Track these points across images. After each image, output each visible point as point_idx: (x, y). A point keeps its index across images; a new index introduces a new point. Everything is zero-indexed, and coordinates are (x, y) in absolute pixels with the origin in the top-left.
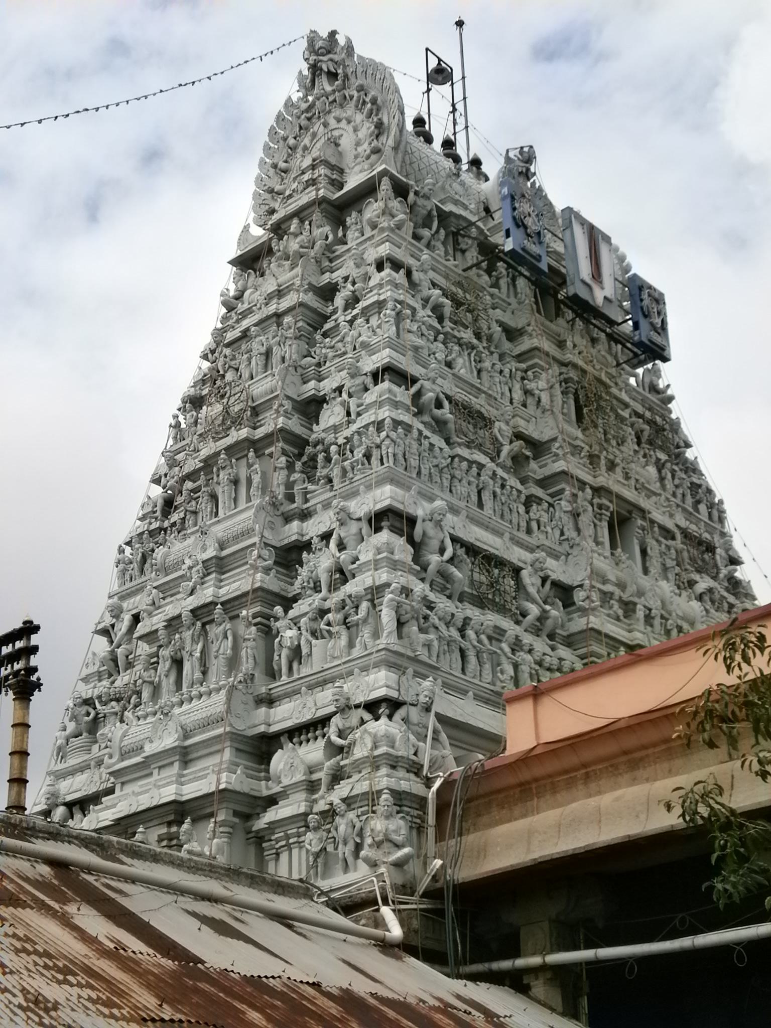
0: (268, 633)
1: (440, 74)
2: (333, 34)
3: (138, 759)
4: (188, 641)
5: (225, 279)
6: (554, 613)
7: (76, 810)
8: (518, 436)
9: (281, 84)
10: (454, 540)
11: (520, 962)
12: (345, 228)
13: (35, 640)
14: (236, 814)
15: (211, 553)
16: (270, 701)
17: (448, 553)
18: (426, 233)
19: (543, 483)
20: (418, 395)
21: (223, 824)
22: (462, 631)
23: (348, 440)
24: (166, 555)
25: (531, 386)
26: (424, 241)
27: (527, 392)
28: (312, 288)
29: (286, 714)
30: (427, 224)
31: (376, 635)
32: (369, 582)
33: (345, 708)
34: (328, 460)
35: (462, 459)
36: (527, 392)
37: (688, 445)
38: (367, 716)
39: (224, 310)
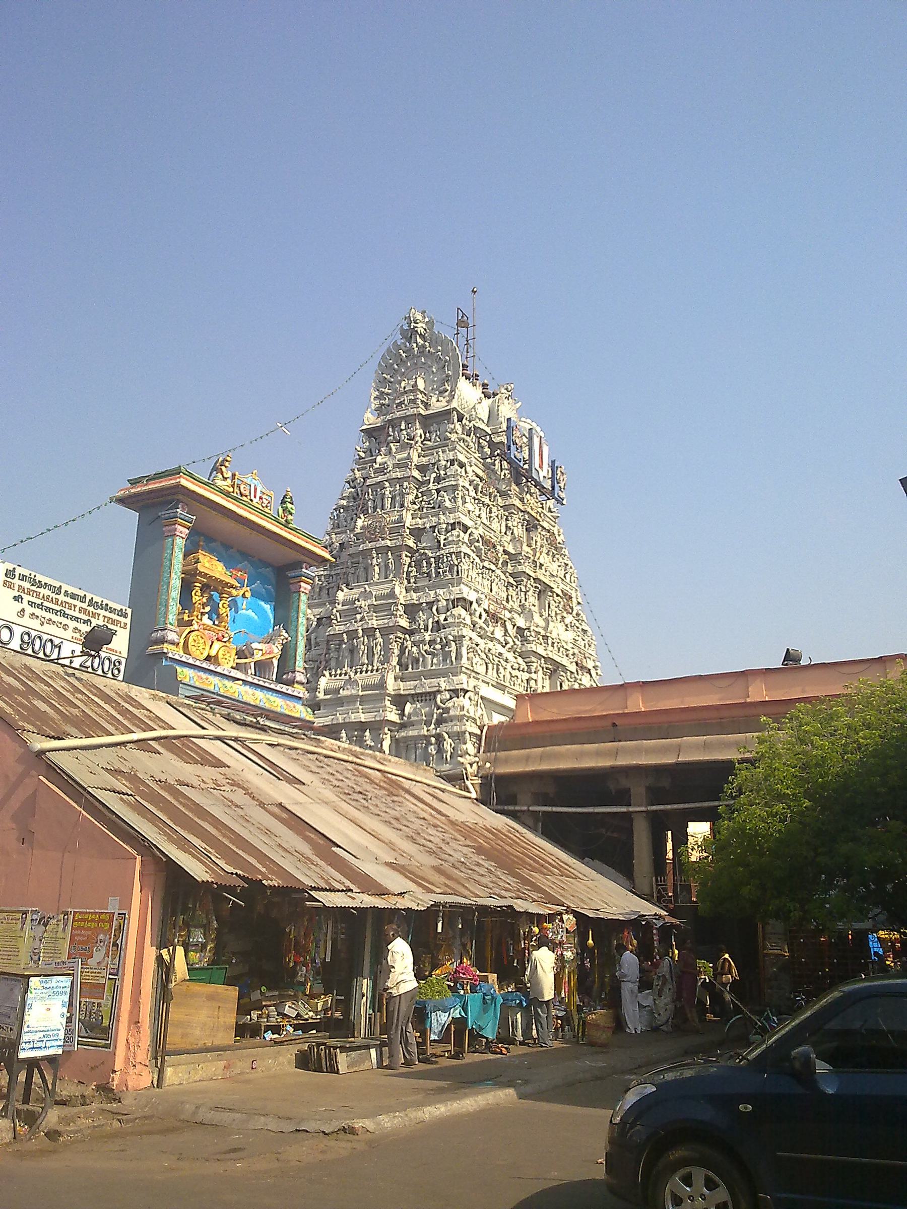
1: (462, 323)
25: (510, 524)
36: (506, 526)
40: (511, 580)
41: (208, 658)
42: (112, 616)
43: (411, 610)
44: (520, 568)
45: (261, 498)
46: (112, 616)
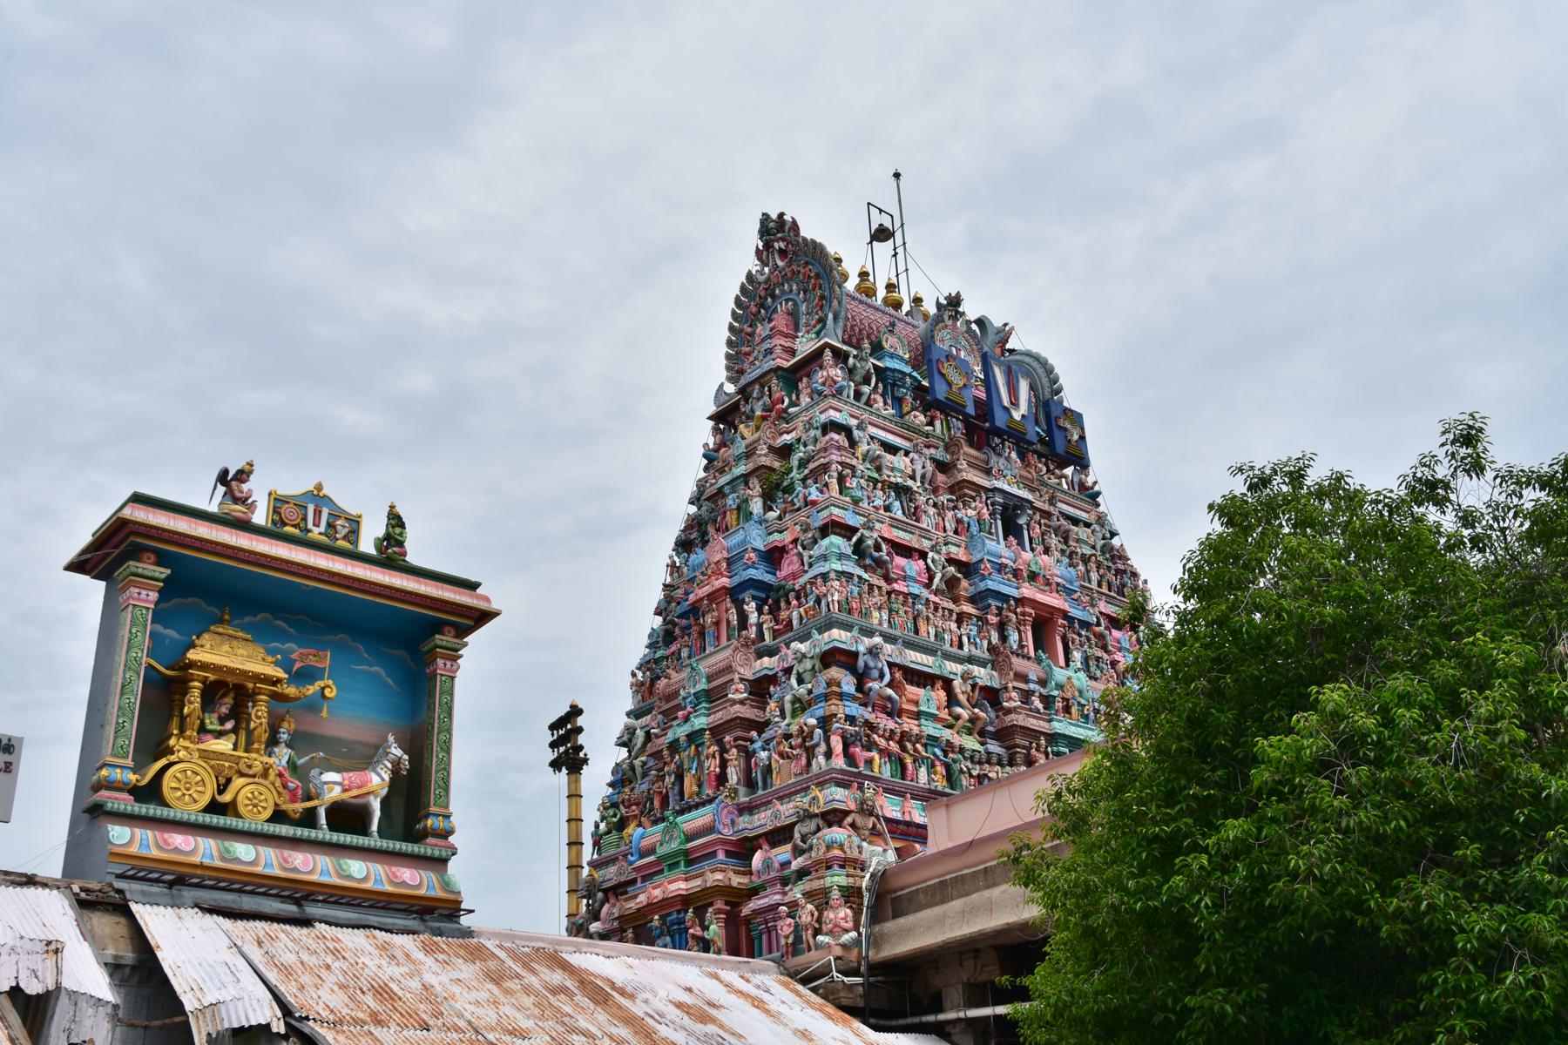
0: (749, 755)
2: (781, 215)
3: (652, 858)
4: (686, 762)
5: (704, 434)
6: (982, 714)
7: (610, 894)
8: (951, 561)
9: (740, 259)
10: (891, 665)
11: (942, 1017)
13: (580, 721)
14: (727, 903)
15: (703, 685)
16: (749, 809)
17: (887, 678)
18: (866, 389)
19: (972, 600)
20: (861, 541)
22: (900, 743)
23: (804, 588)
26: (864, 399)
27: (959, 521)
28: (771, 449)
29: (763, 820)
30: (867, 381)
31: (829, 754)
32: (820, 713)
34: (788, 603)
35: (898, 593)
37: (1113, 534)
38: (821, 823)
39: (705, 462)
40: (968, 608)
41: (214, 807)
43: (761, 688)
44: (982, 586)
45: (329, 525)
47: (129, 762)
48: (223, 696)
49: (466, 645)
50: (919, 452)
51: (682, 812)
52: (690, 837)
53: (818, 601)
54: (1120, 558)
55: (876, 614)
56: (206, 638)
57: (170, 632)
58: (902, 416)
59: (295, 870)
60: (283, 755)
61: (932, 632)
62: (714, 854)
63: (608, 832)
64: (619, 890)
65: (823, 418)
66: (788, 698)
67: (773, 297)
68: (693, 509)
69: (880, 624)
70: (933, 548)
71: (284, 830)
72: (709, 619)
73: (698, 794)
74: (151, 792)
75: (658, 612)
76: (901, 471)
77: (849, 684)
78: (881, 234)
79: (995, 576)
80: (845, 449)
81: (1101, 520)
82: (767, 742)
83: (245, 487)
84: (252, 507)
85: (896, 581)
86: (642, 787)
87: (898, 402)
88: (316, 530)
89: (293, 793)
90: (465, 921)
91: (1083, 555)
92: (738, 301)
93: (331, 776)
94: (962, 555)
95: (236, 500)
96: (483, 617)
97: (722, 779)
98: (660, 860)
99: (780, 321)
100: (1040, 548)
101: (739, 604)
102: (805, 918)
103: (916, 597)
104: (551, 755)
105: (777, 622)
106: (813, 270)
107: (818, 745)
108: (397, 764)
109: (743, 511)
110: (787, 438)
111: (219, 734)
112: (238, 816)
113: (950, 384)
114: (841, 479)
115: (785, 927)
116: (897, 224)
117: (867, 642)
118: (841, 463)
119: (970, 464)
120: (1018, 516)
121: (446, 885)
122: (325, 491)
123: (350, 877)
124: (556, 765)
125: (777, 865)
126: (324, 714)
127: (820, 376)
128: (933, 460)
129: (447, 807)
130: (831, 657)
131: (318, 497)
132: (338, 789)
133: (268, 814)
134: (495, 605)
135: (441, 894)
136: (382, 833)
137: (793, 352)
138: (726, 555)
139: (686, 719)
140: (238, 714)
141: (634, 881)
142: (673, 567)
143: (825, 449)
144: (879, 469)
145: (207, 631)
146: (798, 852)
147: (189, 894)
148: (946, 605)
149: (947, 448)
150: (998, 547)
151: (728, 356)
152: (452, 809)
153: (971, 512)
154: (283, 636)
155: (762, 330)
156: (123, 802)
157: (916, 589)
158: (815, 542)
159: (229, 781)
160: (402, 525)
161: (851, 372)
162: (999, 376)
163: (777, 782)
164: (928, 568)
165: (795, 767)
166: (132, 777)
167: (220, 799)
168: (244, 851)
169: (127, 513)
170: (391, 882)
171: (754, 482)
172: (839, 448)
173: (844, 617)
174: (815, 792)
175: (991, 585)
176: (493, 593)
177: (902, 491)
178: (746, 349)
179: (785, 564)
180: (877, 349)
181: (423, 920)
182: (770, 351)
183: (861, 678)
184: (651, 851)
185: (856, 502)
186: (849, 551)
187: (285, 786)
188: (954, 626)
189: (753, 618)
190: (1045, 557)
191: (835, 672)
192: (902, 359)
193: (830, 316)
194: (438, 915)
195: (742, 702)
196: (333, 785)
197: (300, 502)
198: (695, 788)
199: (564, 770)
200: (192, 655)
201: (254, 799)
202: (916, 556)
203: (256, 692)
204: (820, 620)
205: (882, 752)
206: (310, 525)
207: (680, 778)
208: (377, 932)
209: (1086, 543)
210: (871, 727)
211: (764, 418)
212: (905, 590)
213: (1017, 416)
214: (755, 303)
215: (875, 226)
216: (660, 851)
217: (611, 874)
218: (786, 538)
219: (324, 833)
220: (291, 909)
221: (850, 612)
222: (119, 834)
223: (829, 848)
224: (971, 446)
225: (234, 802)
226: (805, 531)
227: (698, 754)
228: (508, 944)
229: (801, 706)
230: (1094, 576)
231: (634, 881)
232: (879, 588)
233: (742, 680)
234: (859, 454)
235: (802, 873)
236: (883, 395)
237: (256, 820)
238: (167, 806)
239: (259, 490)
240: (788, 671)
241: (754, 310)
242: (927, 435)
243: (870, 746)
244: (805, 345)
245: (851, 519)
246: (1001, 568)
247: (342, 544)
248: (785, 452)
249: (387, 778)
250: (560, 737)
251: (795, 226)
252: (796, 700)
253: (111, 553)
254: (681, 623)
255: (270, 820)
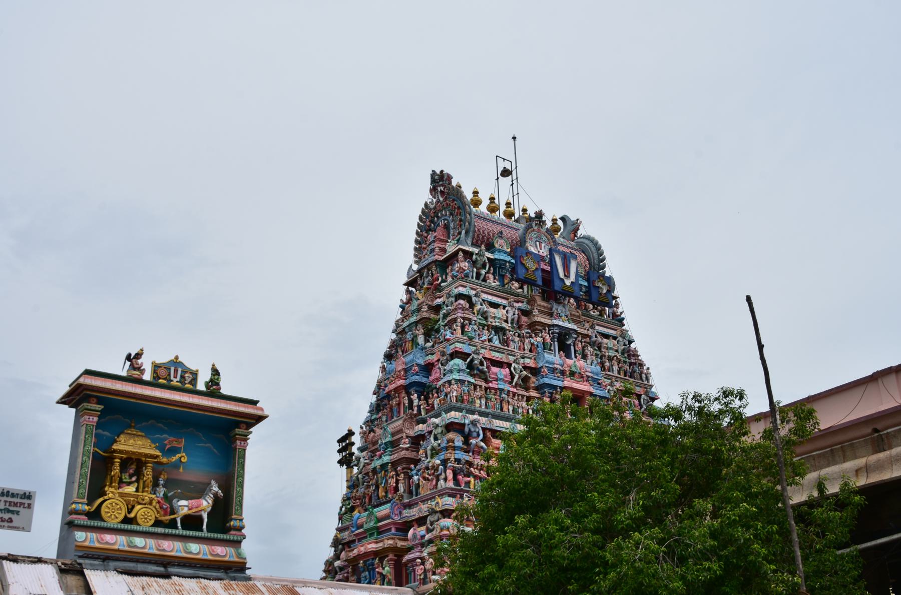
2: (442, 172)
8: (525, 368)
9: (423, 195)
10: (484, 429)
12: (447, 274)
14: (395, 556)
16: (409, 506)
18: (483, 272)
19: (537, 389)
21: (391, 560)
24: (374, 437)
26: (482, 277)
27: (532, 344)
30: (484, 266)
31: (445, 479)
32: (442, 457)
33: (433, 512)
37: (630, 342)
38: (440, 516)
40: (533, 393)
41: (126, 520)
42: (15, 500)
43: (417, 441)
44: (542, 381)
45: (182, 377)
46: (15, 500)
47: (85, 501)
48: (132, 464)
49: (251, 432)
50: (512, 306)
51: (377, 506)
52: (380, 520)
53: (446, 395)
54: (634, 355)
55: (478, 401)
56: (122, 438)
57: (106, 433)
58: (503, 285)
59: (164, 550)
60: (161, 491)
61: (511, 408)
62: (390, 530)
63: (346, 513)
64: (349, 545)
65: (456, 291)
66: (429, 448)
67: (438, 217)
68: (394, 336)
69: (481, 406)
70: (515, 361)
71: (160, 530)
72: (394, 402)
73: (386, 496)
74: (96, 515)
75: (374, 394)
76: (500, 319)
77: (459, 441)
78: (506, 173)
79: (550, 375)
80: (466, 309)
81: (624, 334)
82: (419, 471)
83: (140, 361)
84: (142, 372)
85: (491, 382)
86: (361, 490)
87: (502, 277)
88: (175, 380)
89: (165, 510)
90: (248, 572)
91: (609, 356)
92: (421, 218)
93: (183, 502)
94: (530, 362)
95: (135, 369)
96: (260, 419)
97: (396, 489)
98: (366, 531)
99: (439, 233)
100: (579, 357)
101: (409, 394)
102: (428, 566)
103: (502, 390)
104: (338, 457)
105: (428, 405)
106: (457, 203)
107: (441, 474)
108: (216, 495)
109: (414, 341)
110: (439, 301)
111: (129, 484)
112: (138, 524)
113: (527, 269)
114: (463, 327)
115: (419, 570)
116: (514, 167)
117: (473, 417)
118: (464, 318)
119: (540, 311)
120: (567, 340)
121: (239, 555)
122: (180, 360)
123: (191, 553)
124: (341, 462)
125: (419, 537)
126: (181, 470)
127: (457, 266)
128: (519, 309)
129: (241, 515)
130: (451, 427)
131: (176, 363)
132: (186, 509)
133: (152, 522)
134: (266, 413)
135: (236, 559)
136: (209, 530)
137: (444, 250)
138: (404, 367)
139: (380, 457)
140: (139, 474)
141: (353, 541)
142: (383, 369)
143: (456, 310)
144: (486, 319)
145: (122, 432)
146: (429, 531)
147: (112, 564)
148: (521, 392)
149: (528, 303)
150: (555, 358)
151: (416, 249)
152: (244, 516)
153: (539, 339)
154: (162, 432)
155: (431, 237)
156: (83, 520)
157: (502, 386)
158: (447, 363)
159: (133, 507)
160: (218, 374)
161: (474, 263)
162: (558, 260)
163: (423, 492)
164: (511, 373)
165: (429, 485)
166: (86, 508)
167: (129, 516)
168: (139, 541)
169: (81, 380)
170: (211, 554)
171: (420, 326)
172: (463, 309)
173: (459, 405)
174: (438, 500)
175: (546, 380)
176: (265, 406)
177: (499, 330)
178: (424, 246)
179: (433, 373)
180: (490, 247)
181: (226, 573)
182: (433, 250)
183: (467, 438)
184: (361, 526)
185: (471, 339)
186: (464, 367)
187: (161, 507)
188: (524, 404)
189: (416, 403)
190: (582, 362)
191: (451, 435)
192: (505, 252)
193: (463, 232)
194: (235, 570)
195: (407, 449)
196: (184, 506)
197: (166, 367)
198: (384, 494)
199: (345, 467)
200: (115, 447)
201: (145, 515)
202: (505, 366)
203: (147, 462)
204: (446, 406)
205: (476, 477)
206: (172, 378)
207: (377, 487)
208: (202, 580)
209: (612, 349)
210: (471, 464)
211: (428, 289)
212: (496, 386)
213: (568, 283)
214: (429, 221)
215: (500, 169)
216: (365, 526)
217: (346, 535)
218: (434, 358)
219: (180, 531)
220: (162, 569)
221: (463, 401)
222: (80, 536)
223: (442, 530)
224: (544, 299)
225: (136, 517)
226: (443, 356)
227: (385, 476)
228: (268, 584)
229: (435, 452)
230: (616, 368)
231: (353, 541)
232: (481, 387)
233: (407, 437)
234: (475, 311)
235: (430, 541)
236: (493, 274)
237: (146, 526)
238: (104, 521)
239: (146, 363)
240: (430, 432)
241: (428, 223)
242: (518, 295)
243: (469, 474)
244: (451, 248)
245: (466, 349)
246: (554, 370)
247: (188, 386)
248: (437, 309)
249: (210, 502)
250: (343, 447)
251: (449, 178)
252: (433, 449)
253: (77, 396)
254: (384, 403)
255: (152, 526)
